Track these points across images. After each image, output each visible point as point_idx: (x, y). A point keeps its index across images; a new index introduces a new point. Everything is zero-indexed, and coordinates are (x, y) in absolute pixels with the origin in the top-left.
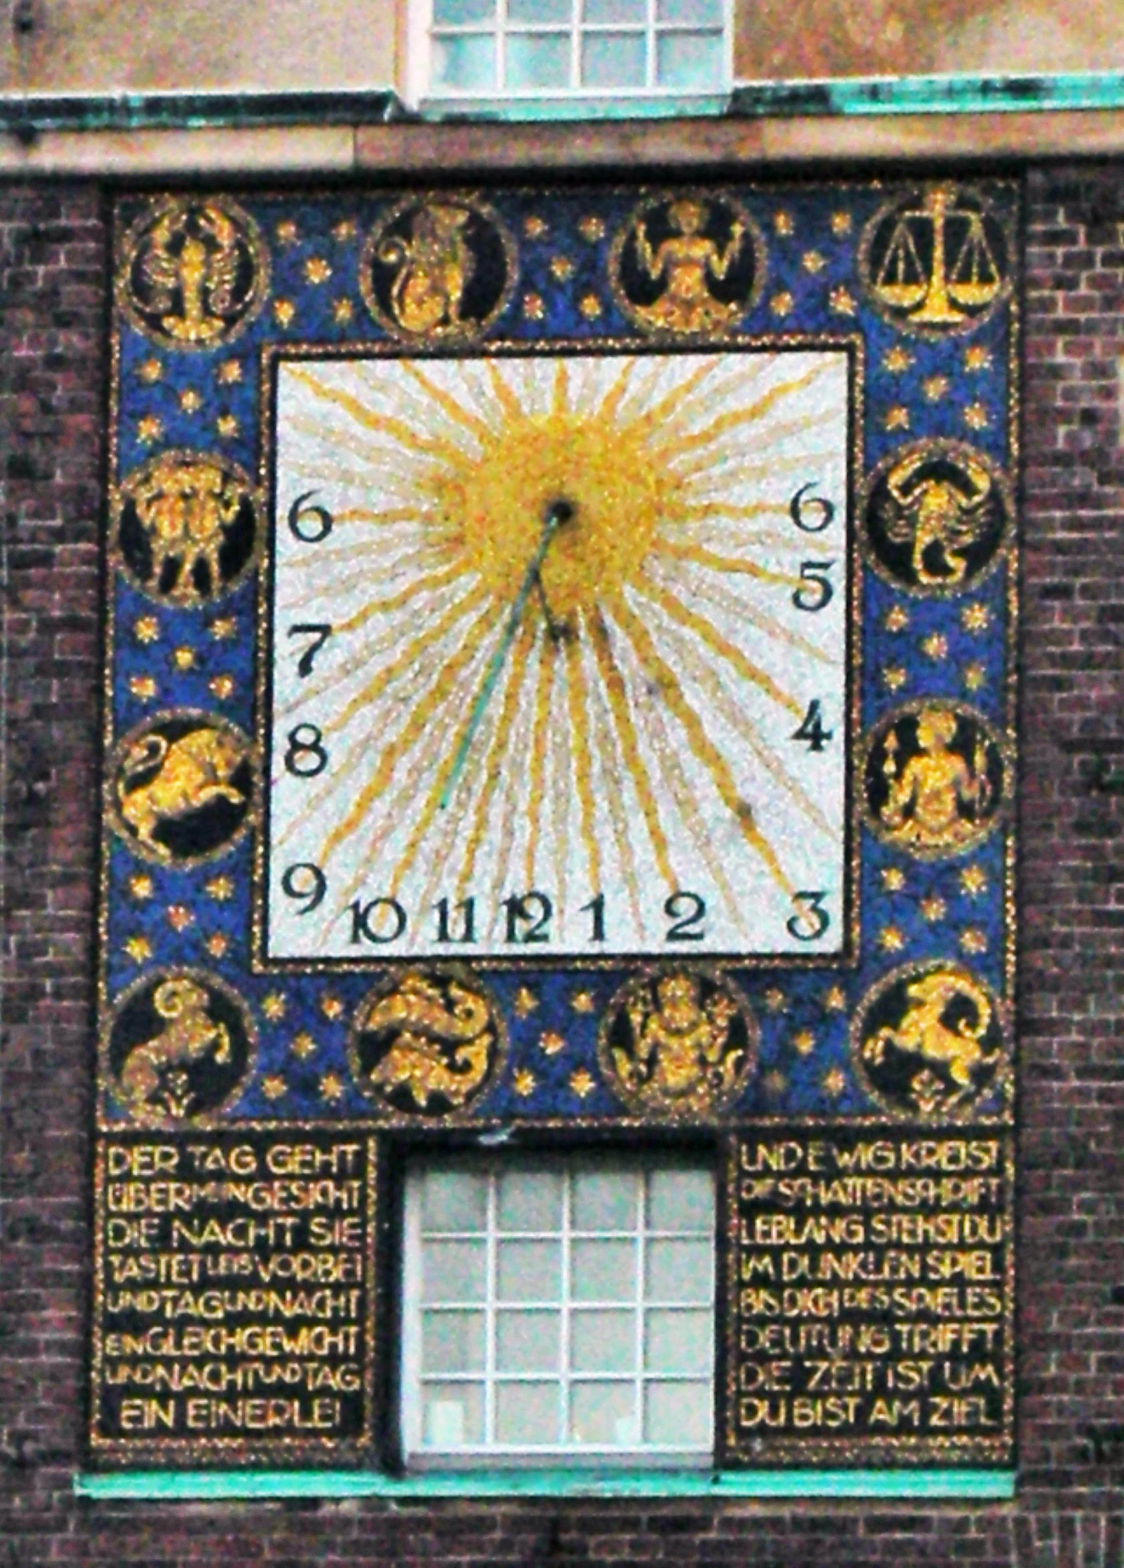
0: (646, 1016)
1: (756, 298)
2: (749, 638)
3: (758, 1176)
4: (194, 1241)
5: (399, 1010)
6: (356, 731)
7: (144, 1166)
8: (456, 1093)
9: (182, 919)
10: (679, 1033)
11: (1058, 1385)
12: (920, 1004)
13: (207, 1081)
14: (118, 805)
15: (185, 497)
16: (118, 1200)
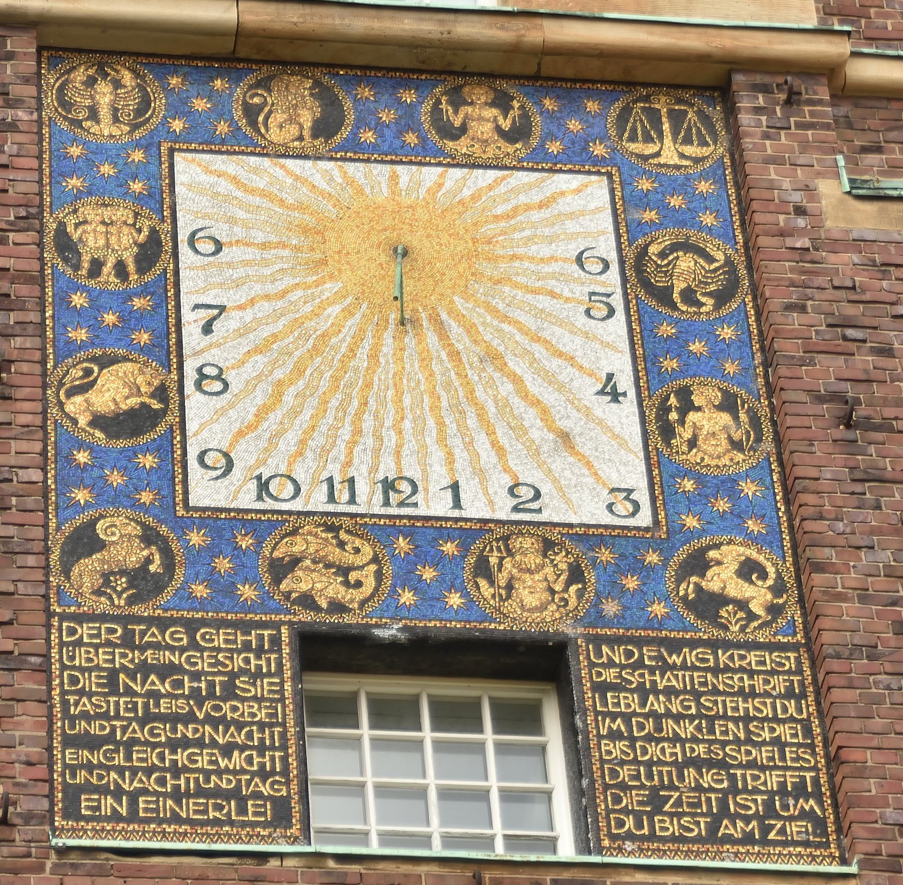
0: (502, 559)
1: (534, 142)
2: (553, 333)
6: (249, 370)
7: (91, 636)
8: (352, 601)
9: (116, 479)
10: (529, 571)
12: (719, 563)
14: (61, 405)
16: (72, 658)
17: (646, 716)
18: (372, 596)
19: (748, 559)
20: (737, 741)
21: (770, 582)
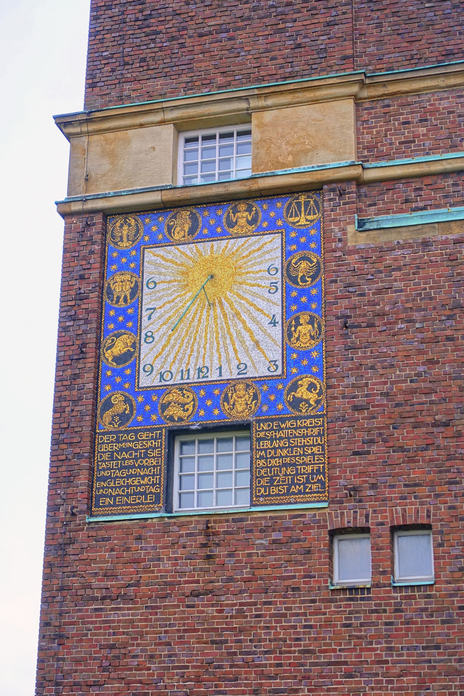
0: (232, 394)
1: (258, 224)
3: (260, 431)
4: (119, 457)
5: (170, 398)
6: (161, 332)
7: (107, 440)
8: (185, 417)
9: (118, 380)
10: (241, 397)
11: (339, 477)
12: (302, 386)
13: (123, 418)
14: (104, 354)
15: (122, 282)
16: (101, 449)
17: (272, 449)
18: (191, 413)
19: (311, 382)
20: (300, 455)
21: (317, 391)
